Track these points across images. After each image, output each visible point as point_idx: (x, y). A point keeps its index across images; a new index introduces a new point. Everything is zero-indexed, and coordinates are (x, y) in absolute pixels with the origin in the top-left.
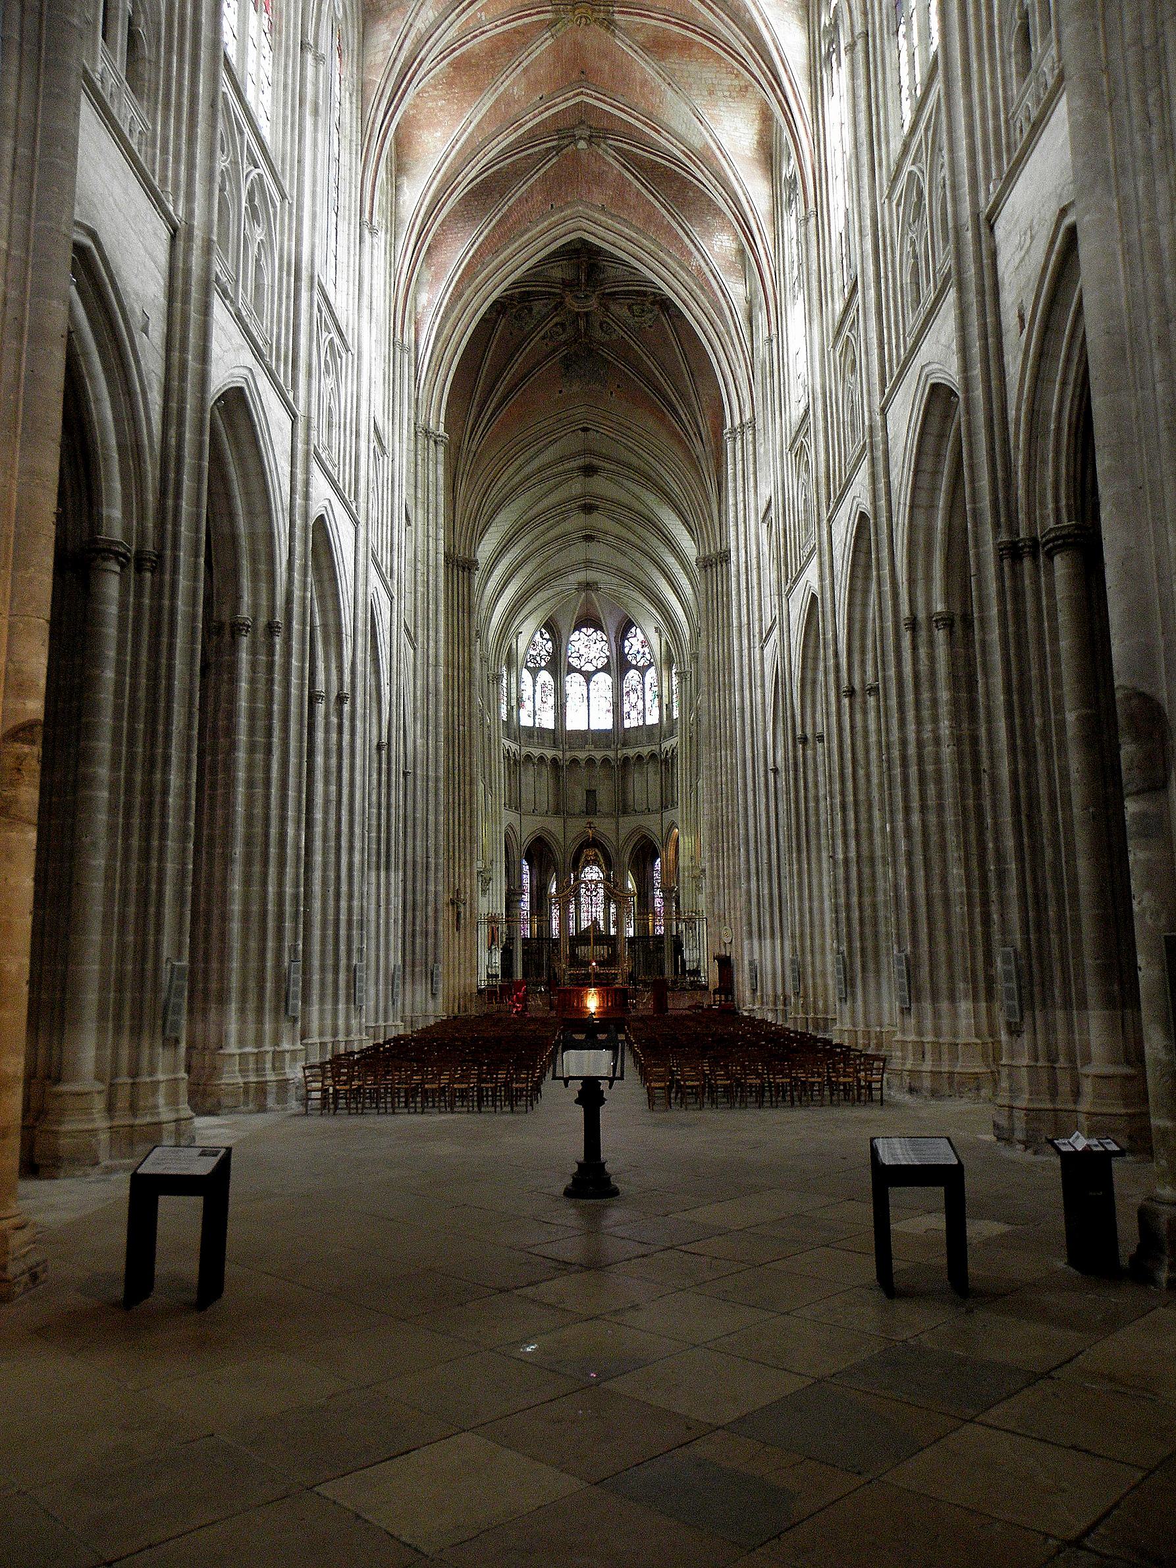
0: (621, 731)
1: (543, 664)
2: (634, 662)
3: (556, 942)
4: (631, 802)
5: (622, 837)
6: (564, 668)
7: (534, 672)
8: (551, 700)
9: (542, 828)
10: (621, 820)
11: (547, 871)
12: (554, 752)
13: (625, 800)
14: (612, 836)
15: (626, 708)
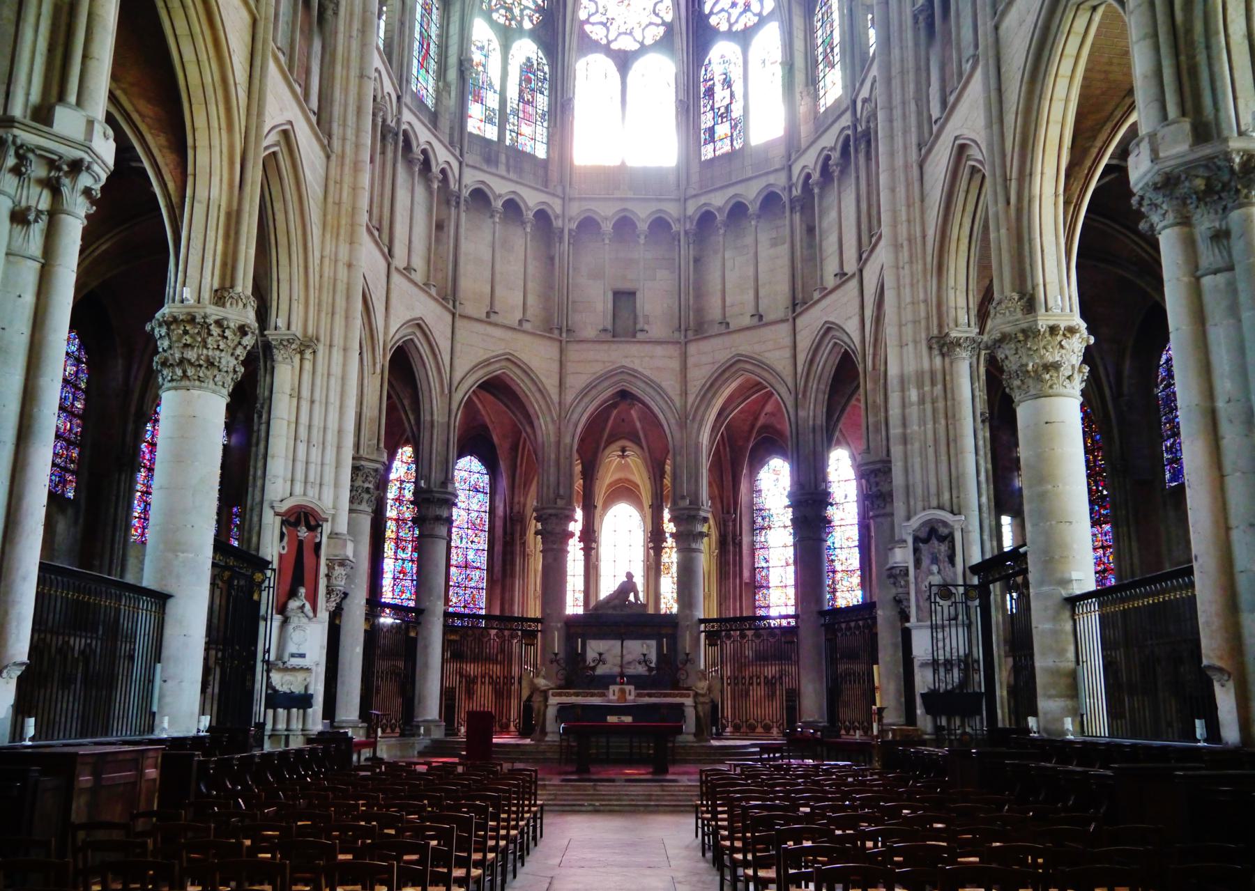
0: (695, 169)
1: (527, 25)
2: (724, 27)
3: (528, 631)
4: (715, 312)
5: (694, 388)
6: (572, 41)
7: (507, 35)
8: (542, 101)
9: (510, 360)
10: (692, 348)
11: (527, 484)
12: (543, 197)
13: (700, 311)
14: (670, 384)
15: (707, 120)
